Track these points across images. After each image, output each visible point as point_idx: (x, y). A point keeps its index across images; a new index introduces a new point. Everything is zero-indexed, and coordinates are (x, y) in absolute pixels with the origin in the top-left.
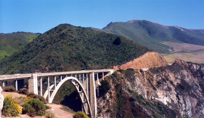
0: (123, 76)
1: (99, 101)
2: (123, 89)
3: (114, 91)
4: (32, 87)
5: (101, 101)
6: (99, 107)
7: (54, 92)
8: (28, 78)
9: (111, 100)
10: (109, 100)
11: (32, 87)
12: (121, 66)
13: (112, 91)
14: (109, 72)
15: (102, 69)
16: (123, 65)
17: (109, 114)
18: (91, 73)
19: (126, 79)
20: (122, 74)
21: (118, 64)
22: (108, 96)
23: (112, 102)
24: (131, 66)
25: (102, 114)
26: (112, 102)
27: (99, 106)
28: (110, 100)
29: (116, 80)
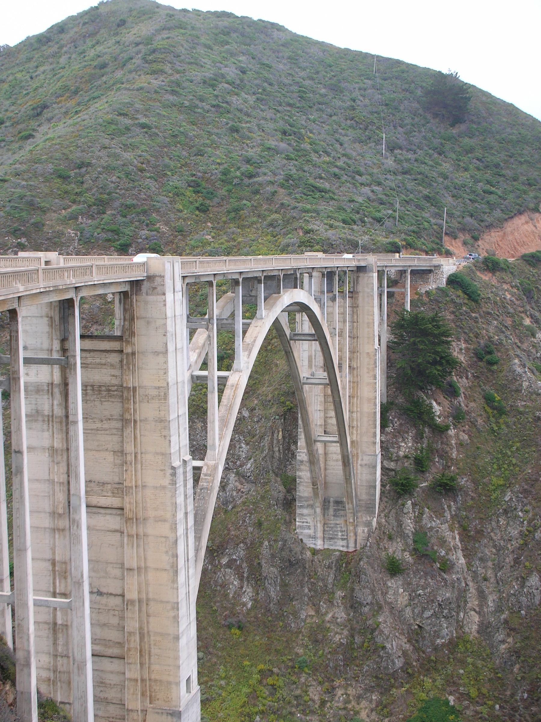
0: (509, 296)
1: (389, 429)
2: (519, 370)
3: (464, 379)
4: (157, 353)
5: (400, 433)
6: (392, 465)
7: (230, 382)
8: (127, 288)
9: (455, 427)
10: (447, 428)
11: (157, 353)
12: (480, 243)
13: (455, 378)
14: (438, 267)
15: (395, 249)
16: (486, 237)
17: (449, 507)
18: (360, 269)
19: (525, 312)
20: (505, 287)
21: (463, 230)
22: (439, 404)
23: (461, 444)
24: (525, 239)
25: (414, 505)
26: (461, 444)
27: (390, 459)
28: (452, 432)
29: (476, 320)
